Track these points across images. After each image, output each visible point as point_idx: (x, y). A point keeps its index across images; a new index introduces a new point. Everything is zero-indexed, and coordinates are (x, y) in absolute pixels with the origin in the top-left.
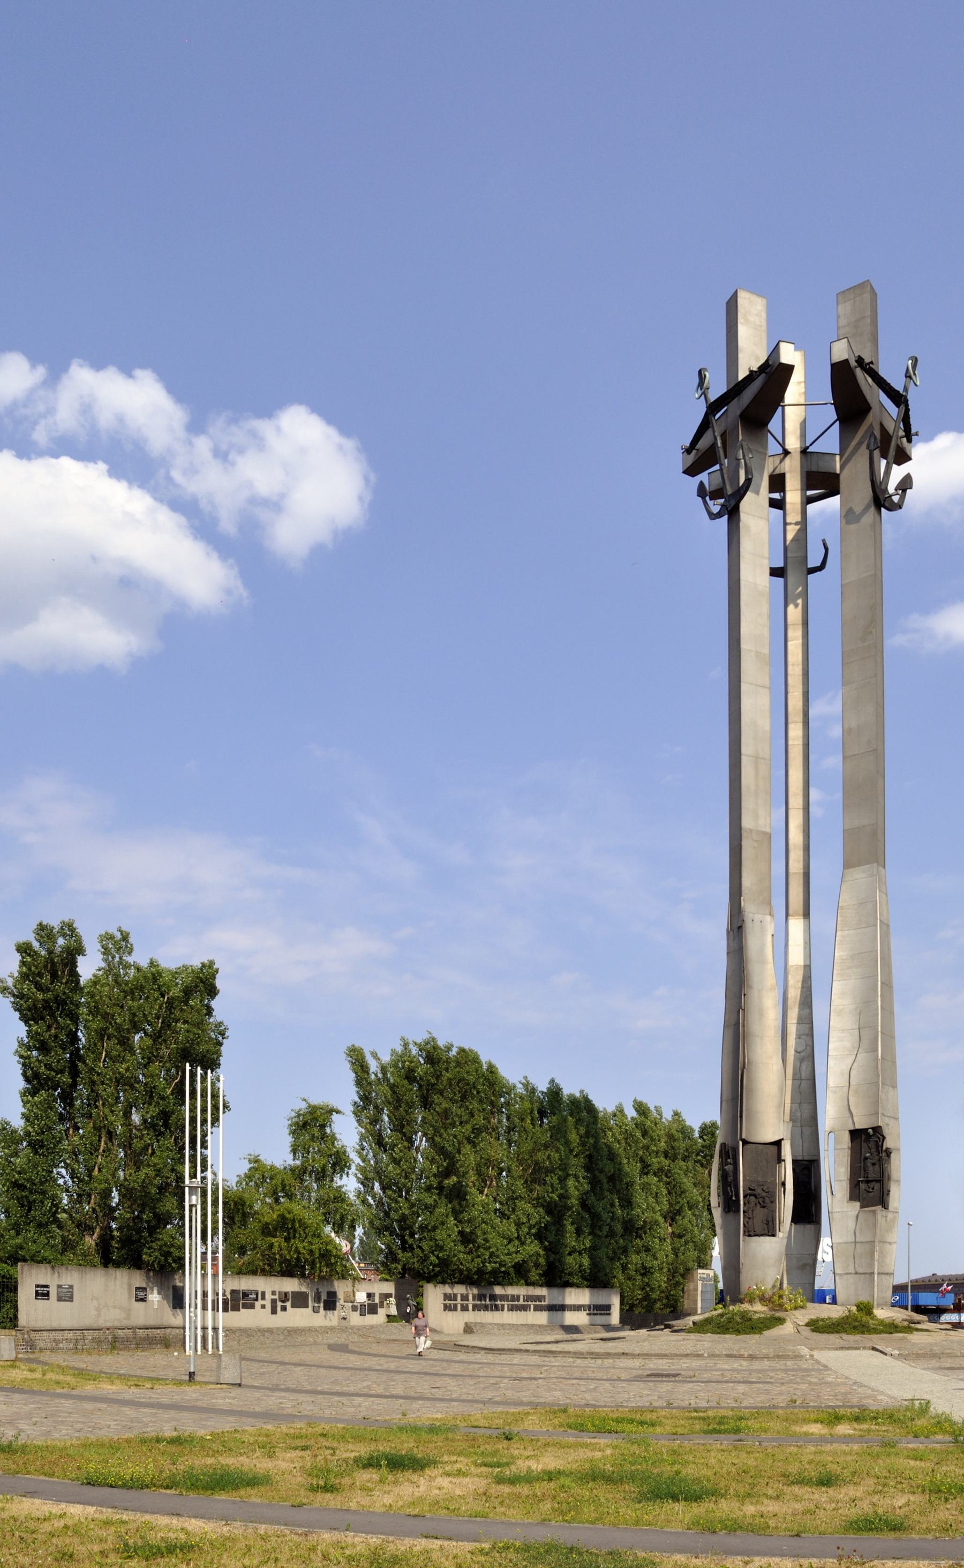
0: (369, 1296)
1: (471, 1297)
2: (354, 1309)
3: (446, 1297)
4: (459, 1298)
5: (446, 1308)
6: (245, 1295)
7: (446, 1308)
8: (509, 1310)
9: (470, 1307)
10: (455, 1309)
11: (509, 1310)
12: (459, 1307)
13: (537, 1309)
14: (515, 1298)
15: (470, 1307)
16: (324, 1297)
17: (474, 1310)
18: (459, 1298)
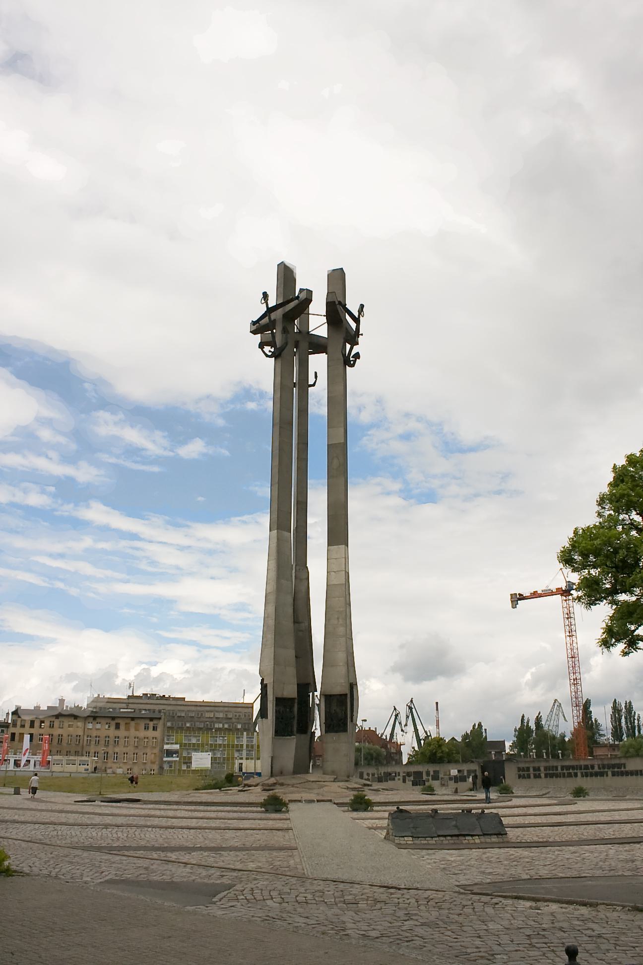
0: (459, 771)
1: (542, 769)
2: (451, 779)
3: (519, 769)
4: (531, 770)
5: (520, 777)
6: (390, 774)
7: (520, 777)
8: (582, 776)
9: (543, 775)
10: (529, 777)
11: (582, 776)
12: (532, 776)
13: (613, 775)
14: (586, 767)
15: (543, 775)
16: (432, 773)
17: (546, 776)
18: (531, 770)
